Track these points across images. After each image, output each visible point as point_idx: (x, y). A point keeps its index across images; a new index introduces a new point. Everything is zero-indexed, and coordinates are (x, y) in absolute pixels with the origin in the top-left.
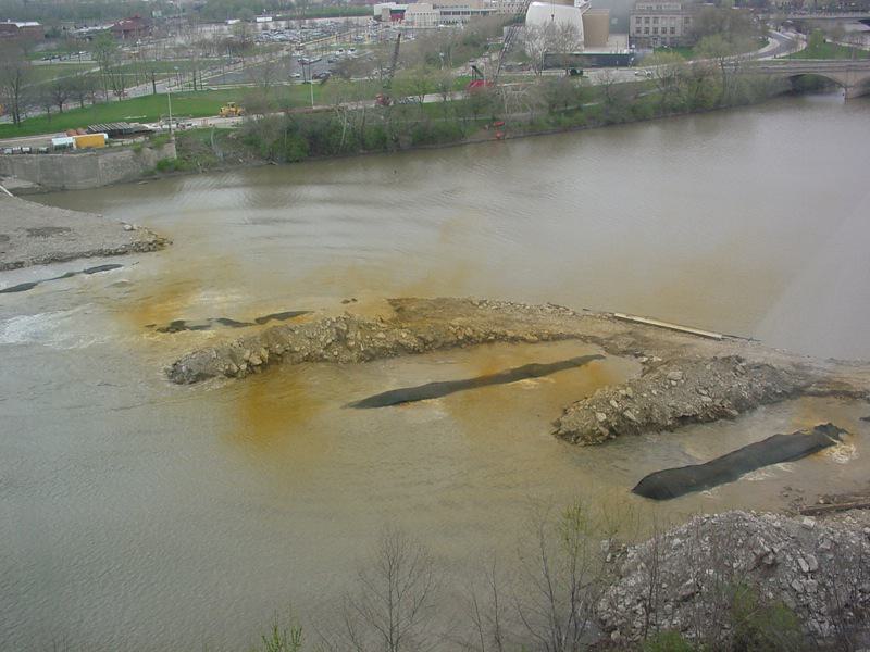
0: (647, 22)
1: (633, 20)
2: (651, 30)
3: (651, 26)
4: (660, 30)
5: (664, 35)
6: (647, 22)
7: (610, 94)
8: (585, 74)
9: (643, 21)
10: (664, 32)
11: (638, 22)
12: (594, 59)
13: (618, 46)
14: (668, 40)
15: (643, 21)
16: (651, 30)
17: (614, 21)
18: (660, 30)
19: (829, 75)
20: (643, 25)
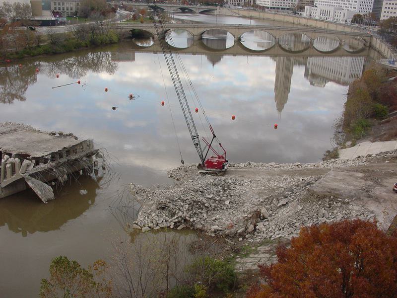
0: (59, 4)
1: (52, 4)
2: (61, 9)
3: (61, 6)
4: (65, 9)
5: (67, 11)
6: (59, 4)
7: (55, 40)
8: (36, 29)
9: (57, 4)
10: (67, 10)
11: (55, 5)
12: (41, 22)
13: (48, 16)
14: (70, 14)
15: (57, 4)
16: (61, 9)
17: (43, 4)
18: (65, 9)
19: (147, 30)
20: (57, 6)
